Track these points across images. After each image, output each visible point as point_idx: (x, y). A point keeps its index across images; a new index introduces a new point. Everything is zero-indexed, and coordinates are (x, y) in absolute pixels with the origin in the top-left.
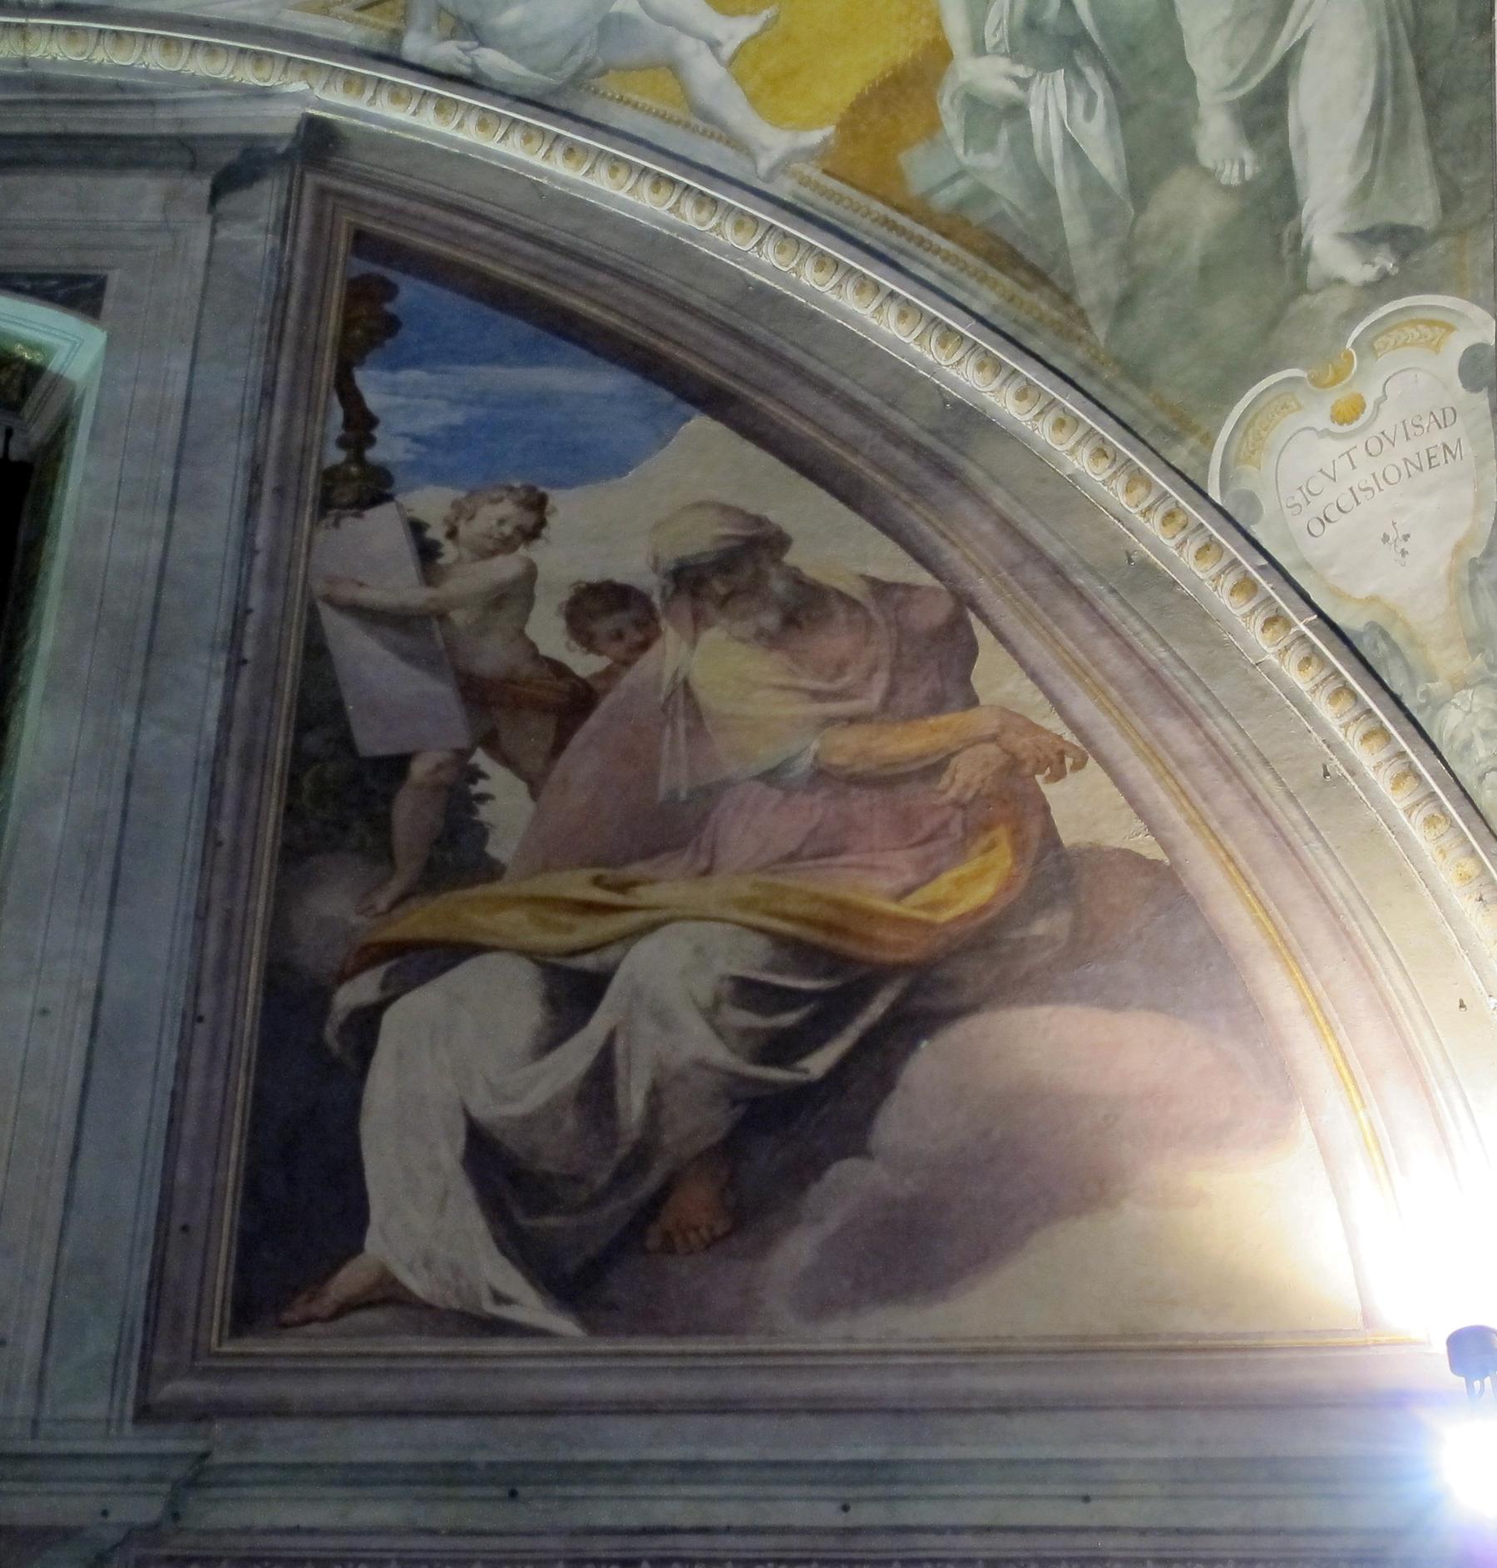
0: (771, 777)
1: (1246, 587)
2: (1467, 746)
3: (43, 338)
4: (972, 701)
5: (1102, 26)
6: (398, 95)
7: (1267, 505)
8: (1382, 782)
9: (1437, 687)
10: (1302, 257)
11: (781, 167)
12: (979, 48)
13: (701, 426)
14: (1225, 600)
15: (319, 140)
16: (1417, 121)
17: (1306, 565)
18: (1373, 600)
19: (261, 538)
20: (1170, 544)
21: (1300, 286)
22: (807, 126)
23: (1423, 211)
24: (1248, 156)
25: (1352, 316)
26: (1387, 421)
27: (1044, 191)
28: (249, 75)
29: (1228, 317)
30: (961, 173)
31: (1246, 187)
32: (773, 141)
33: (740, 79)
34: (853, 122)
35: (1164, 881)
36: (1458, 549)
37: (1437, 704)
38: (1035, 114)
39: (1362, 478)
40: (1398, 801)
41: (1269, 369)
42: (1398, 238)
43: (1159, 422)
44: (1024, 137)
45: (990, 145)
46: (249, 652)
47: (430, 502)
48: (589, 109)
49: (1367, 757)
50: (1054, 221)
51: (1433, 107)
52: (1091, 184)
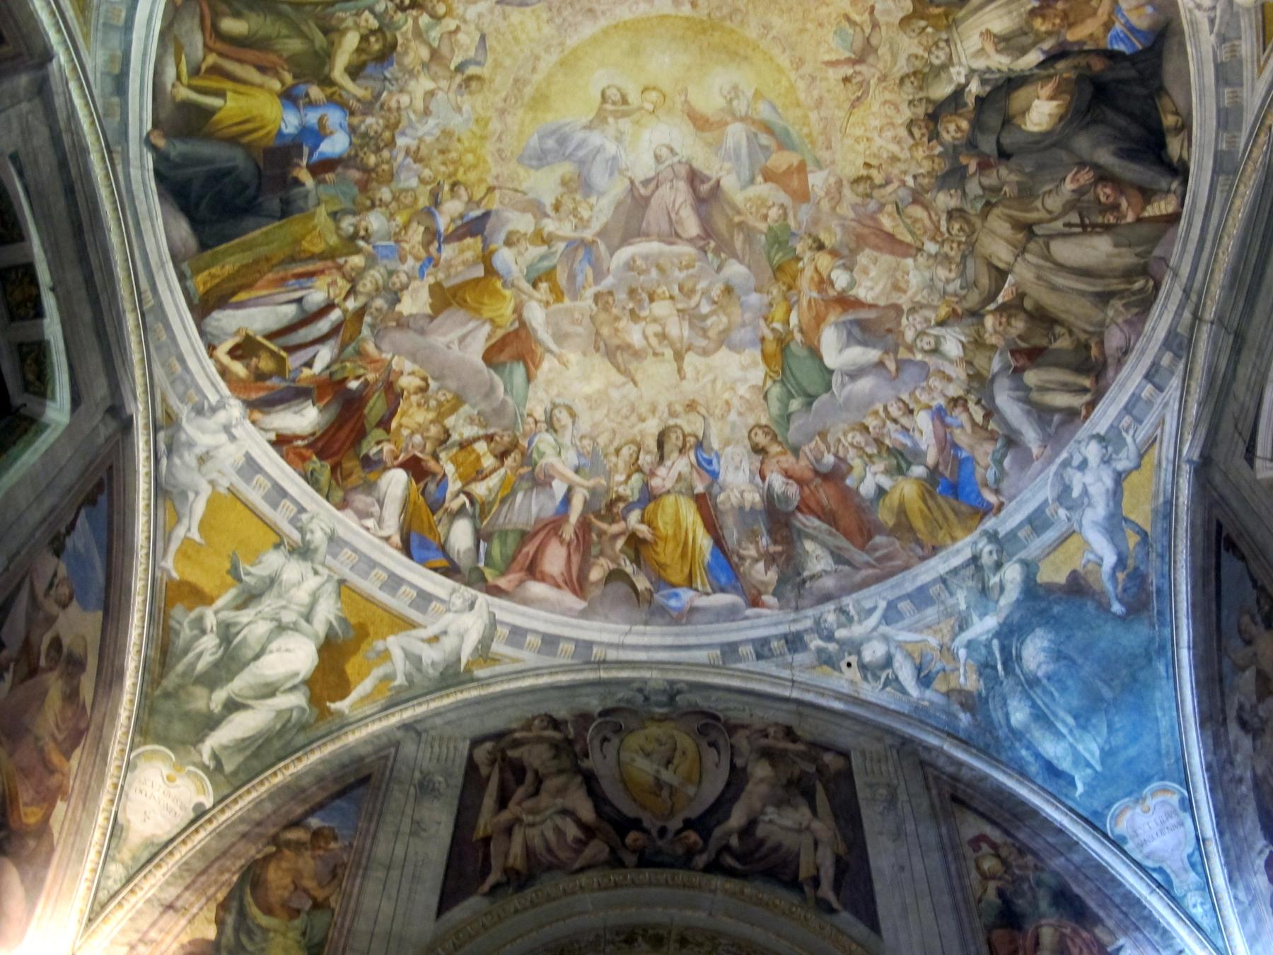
0: (37, 739)
1: (115, 786)
2: (109, 877)
3: (58, 396)
4: (68, 759)
5: (236, 647)
6: (147, 442)
7: (137, 772)
8: (89, 865)
9: (118, 856)
10: (202, 740)
11: (164, 570)
12: (216, 613)
13: (100, 614)
14: (109, 783)
15: (127, 426)
16: (248, 752)
17: (127, 795)
18: (129, 821)
19: (37, 535)
20: (115, 754)
21: (195, 745)
22: (176, 569)
23: (229, 767)
24: (219, 708)
25: (195, 764)
26: (174, 792)
27: (186, 652)
28: (139, 390)
29: (178, 728)
30: (180, 623)
31: (211, 712)
32: (169, 563)
33: (182, 543)
34: (183, 584)
35: (52, 850)
36: (153, 835)
37: (114, 859)
38: (205, 638)
39: (157, 794)
40: (87, 874)
41: (171, 749)
42: (219, 766)
43: (143, 731)
44: (196, 638)
45: (191, 629)
46: (12, 567)
47: (63, 570)
48: (160, 502)
49: (92, 855)
50: (179, 659)
51: (255, 755)
52: (192, 665)
